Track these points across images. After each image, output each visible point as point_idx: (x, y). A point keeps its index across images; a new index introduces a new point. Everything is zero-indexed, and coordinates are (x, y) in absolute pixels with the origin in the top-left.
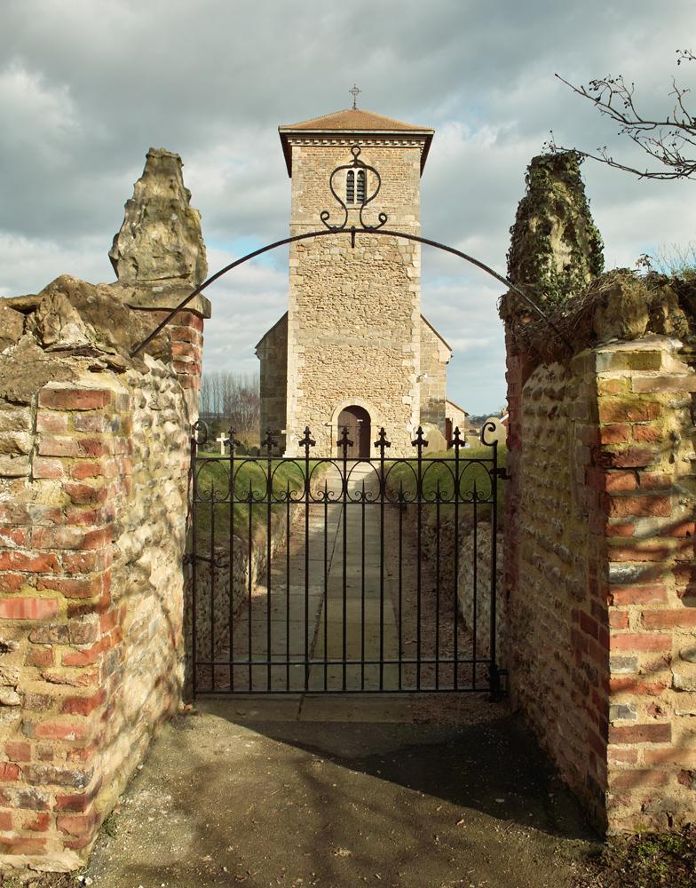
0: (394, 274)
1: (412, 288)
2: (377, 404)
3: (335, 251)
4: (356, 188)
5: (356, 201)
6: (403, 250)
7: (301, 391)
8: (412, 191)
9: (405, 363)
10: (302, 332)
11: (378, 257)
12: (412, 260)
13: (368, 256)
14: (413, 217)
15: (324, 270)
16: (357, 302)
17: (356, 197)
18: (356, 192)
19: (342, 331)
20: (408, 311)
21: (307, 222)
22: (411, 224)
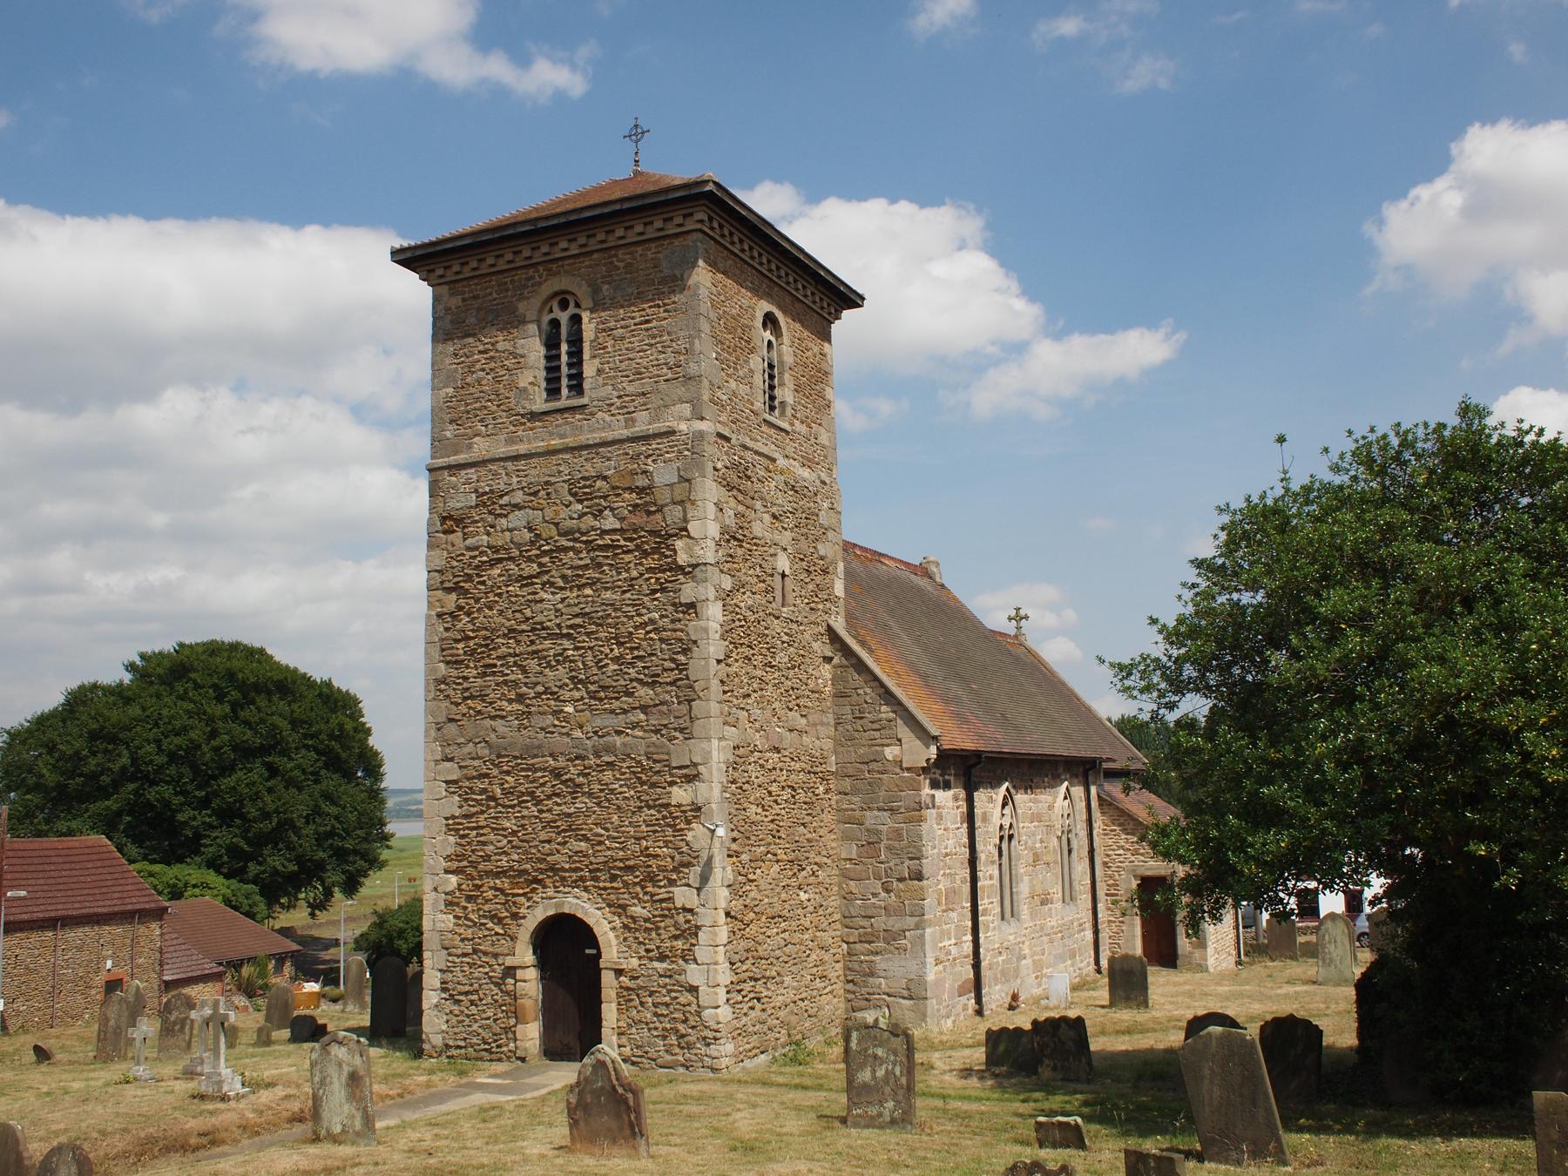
0: (649, 562)
1: (688, 592)
2: (620, 909)
3: (518, 519)
4: (564, 358)
5: (565, 391)
6: (663, 496)
7: (453, 880)
8: (681, 344)
9: (680, 795)
10: (451, 729)
11: (610, 522)
12: (685, 520)
13: (589, 521)
14: (686, 409)
15: (497, 571)
16: (567, 643)
17: (565, 382)
18: (565, 370)
19: (538, 721)
20: (682, 658)
21: (462, 458)
22: (683, 427)
